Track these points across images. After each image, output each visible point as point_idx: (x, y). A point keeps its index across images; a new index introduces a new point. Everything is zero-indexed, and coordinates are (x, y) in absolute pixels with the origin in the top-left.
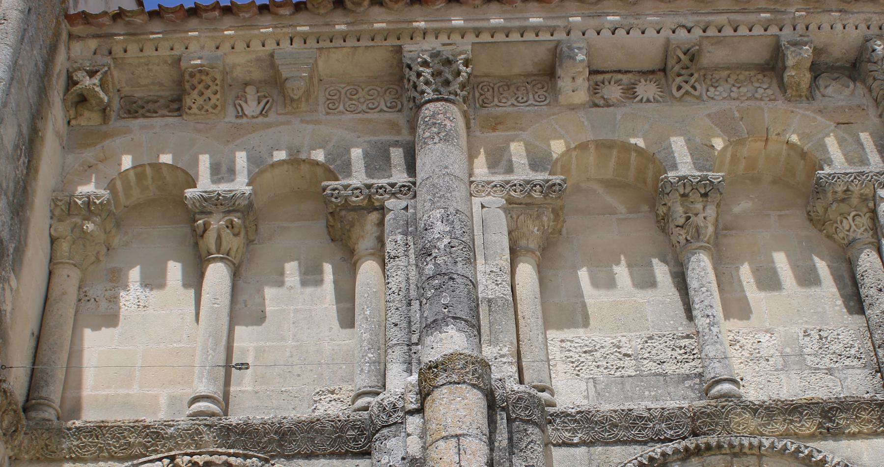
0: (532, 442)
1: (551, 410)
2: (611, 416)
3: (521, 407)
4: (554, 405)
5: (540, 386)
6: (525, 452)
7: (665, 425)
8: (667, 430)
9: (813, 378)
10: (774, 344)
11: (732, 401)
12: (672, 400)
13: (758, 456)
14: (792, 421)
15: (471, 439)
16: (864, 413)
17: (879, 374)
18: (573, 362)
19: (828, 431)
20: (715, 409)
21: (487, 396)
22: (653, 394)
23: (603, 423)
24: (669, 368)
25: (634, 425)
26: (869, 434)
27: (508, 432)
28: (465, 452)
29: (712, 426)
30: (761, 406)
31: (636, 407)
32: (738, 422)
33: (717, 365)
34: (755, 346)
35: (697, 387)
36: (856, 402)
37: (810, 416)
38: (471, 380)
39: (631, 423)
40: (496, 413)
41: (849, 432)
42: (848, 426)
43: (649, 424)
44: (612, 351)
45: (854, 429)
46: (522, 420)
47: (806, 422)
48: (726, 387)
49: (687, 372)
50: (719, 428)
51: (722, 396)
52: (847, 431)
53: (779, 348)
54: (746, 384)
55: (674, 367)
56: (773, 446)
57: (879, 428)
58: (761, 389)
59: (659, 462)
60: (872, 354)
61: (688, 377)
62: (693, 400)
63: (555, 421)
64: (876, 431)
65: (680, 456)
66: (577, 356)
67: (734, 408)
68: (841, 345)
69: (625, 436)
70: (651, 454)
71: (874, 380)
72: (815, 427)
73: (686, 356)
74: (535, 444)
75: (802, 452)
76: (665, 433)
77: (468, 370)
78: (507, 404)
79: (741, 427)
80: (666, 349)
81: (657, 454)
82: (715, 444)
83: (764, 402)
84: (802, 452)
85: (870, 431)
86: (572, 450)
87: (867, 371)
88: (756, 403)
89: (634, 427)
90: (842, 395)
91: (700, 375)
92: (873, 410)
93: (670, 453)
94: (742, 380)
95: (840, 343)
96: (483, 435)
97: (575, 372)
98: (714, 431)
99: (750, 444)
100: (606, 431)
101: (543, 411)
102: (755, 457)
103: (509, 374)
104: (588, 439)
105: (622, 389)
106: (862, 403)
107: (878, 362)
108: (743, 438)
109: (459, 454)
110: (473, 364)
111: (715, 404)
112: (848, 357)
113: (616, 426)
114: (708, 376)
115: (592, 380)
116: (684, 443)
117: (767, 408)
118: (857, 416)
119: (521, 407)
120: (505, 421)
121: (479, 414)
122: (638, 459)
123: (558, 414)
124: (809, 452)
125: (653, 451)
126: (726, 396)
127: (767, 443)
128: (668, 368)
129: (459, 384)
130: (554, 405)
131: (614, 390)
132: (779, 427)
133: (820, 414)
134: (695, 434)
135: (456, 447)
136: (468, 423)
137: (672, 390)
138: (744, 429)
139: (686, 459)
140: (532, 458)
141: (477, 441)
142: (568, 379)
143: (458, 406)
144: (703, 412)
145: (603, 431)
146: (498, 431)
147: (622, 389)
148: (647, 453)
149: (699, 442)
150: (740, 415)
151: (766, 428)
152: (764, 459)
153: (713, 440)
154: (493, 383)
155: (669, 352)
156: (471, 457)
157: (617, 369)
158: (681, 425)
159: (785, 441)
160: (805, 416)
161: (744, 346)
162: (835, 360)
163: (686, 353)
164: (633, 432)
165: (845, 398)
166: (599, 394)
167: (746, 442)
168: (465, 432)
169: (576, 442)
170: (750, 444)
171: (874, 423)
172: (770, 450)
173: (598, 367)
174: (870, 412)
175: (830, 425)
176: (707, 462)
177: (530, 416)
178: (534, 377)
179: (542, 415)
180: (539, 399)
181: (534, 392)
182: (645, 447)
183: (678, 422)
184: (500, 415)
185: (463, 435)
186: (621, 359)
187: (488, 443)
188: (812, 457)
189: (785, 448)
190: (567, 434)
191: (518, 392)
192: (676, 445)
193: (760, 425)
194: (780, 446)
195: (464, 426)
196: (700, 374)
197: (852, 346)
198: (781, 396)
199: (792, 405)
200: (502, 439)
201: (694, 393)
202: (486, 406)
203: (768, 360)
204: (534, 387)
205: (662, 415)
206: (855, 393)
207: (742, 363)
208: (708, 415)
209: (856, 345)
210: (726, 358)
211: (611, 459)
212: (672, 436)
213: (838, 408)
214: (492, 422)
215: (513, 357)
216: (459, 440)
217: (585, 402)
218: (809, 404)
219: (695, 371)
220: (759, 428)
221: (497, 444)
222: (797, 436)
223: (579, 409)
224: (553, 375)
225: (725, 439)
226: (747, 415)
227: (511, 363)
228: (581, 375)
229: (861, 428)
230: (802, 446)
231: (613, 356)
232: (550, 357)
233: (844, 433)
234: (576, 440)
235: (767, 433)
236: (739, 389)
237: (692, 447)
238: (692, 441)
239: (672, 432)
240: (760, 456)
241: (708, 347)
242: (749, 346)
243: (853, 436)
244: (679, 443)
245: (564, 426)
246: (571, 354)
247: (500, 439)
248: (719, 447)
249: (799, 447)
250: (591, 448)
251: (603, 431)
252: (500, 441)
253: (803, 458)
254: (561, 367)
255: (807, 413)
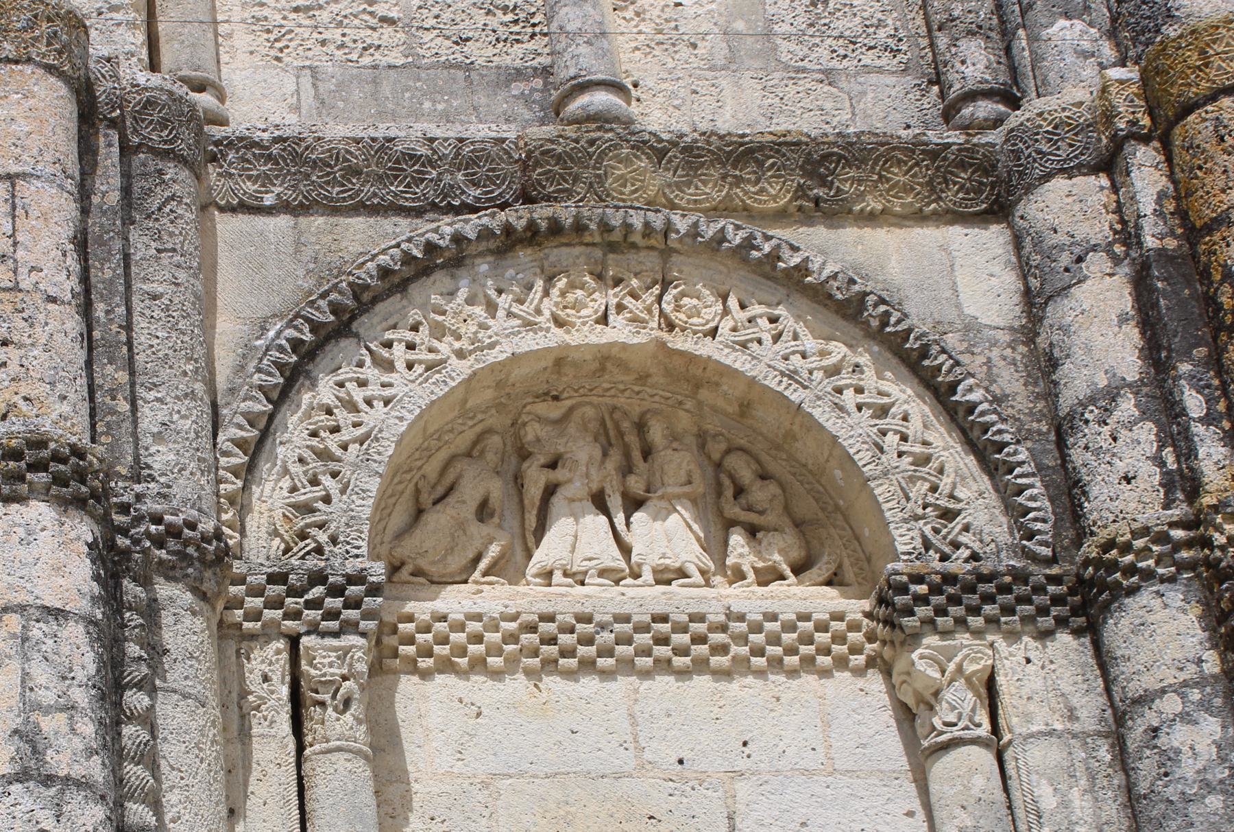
0: (172, 198)
1: (217, 132)
2: (348, 152)
3: (151, 122)
4: (223, 122)
5: (196, 78)
6: (157, 220)
7: (465, 175)
8: (467, 186)
9: (792, 89)
10: (709, 12)
11: (611, 130)
12: (481, 122)
13: (662, 252)
14: (738, 181)
15: (39, 185)
16: (896, 171)
17: (936, 89)
18: (268, 31)
19: (817, 204)
20: (573, 145)
21: (77, 92)
22: (440, 107)
23: (329, 166)
24: (479, 52)
25: (396, 174)
26: (904, 217)
27: (122, 176)
28: (26, 212)
29: (566, 181)
30: (675, 144)
31: (402, 134)
32: (622, 176)
33: (584, 49)
34: (669, 13)
35: (537, 96)
36: (882, 145)
37: (778, 170)
38: (44, 56)
39: (390, 169)
40: (97, 133)
41: (862, 210)
42: (861, 196)
43: (427, 173)
44: (354, 11)
45: (873, 203)
46: (152, 150)
47: (770, 183)
48: (600, 99)
49: (518, 63)
50: (580, 188)
51: (590, 118)
52: (857, 208)
53: (722, 21)
54: (643, 97)
55: (490, 51)
56: (694, 232)
57: (928, 204)
58: (677, 108)
59: (447, 254)
60: (924, 42)
61: (519, 74)
62: (527, 123)
63: (224, 156)
64: (921, 210)
65: (492, 244)
66: (278, 17)
67: (615, 146)
68: (857, 20)
69: (375, 195)
70: (429, 235)
71: (925, 100)
72: (789, 196)
73: (516, 29)
74: (180, 202)
75: (758, 248)
76: (463, 192)
77: (37, 33)
78: (122, 114)
79: (629, 188)
80: (474, 11)
81: (442, 238)
82: (570, 221)
83: (681, 136)
84: (758, 248)
85: (908, 210)
86: (260, 221)
87: (910, 80)
88: (665, 136)
89: (396, 177)
90: (851, 130)
91: (546, 71)
92: (917, 164)
93: (472, 235)
94: (635, 85)
95: (855, 15)
96: (67, 177)
97: (273, 53)
98: (569, 193)
99: (647, 224)
100: (335, 182)
101: (199, 132)
102: (655, 253)
103: (127, 48)
104: (295, 199)
105: (375, 95)
106: (894, 149)
107: (935, 61)
108: (631, 212)
109: (14, 217)
110: (49, 20)
111: (574, 136)
112: (871, 48)
113: (358, 173)
114: (564, 74)
115: (308, 72)
116: (502, 216)
117: (688, 149)
118: (881, 176)
119: (151, 122)
120: (116, 150)
121: (59, 130)
122: (403, 246)
123: (231, 143)
124: (773, 249)
125: (436, 231)
126: (600, 119)
127: (682, 224)
128: (476, 52)
129: (17, 62)
130: (223, 122)
131: (357, 95)
132: (711, 191)
133: (802, 168)
134: (528, 199)
135: (6, 200)
136: (35, 152)
137: (483, 100)
138: (636, 191)
139: (506, 251)
140: (171, 234)
141: (54, 191)
142: (257, 68)
143: (14, 113)
144: (548, 151)
145: (328, 183)
146: (99, 173)
147: (375, 95)
148: (423, 235)
149: (535, 216)
150: (627, 161)
151: (683, 192)
152: (675, 258)
153: (566, 212)
154: (92, 65)
155: (480, 18)
156: (40, 224)
157: (365, 49)
158: (498, 177)
159: (722, 223)
160: (769, 169)
161: (644, 11)
162: (842, 52)
163: (516, 22)
164: (392, 188)
165: (858, 135)
166: (323, 103)
167: (637, 221)
168: (28, 169)
169: (268, 203)
170: (647, 224)
171: (918, 194)
172: (688, 240)
173: (323, 43)
174: (911, 168)
175: (820, 192)
176: (552, 259)
177: (171, 142)
178: (184, 58)
179: (197, 142)
180: (193, 107)
181: (181, 90)
182: (419, 221)
183: (493, 170)
184: (106, 135)
185: (23, 176)
186: (374, 29)
187: (77, 196)
188: (779, 259)
189: (721, 237)
190: (250, 187)
191: (146, 89)
192: (485, 220)
193: (669, 186)
194: (711, 233)
195: (25, 157)
196: (545, 68)
197: (880, 24)
198: (719, 124)
199: (742, 144)
200: (108, 189)
201: (530, 109)
202: (75, 115)
203: (694, 46)
204: (182, 79)
205: (457, 154)
206: (880, 127)
207: (637, 49)
208: (559, 159)
209: (890, 22)
210: (603, 34)
211: (344, 244)
212: (477, 199)
213: (841, 157)
214: (87, 151)
215: (137, 11)
216: (13, 186)
217: (292, 119)
218: (780, 144)
219: (535, 63)
220: (667, 191)
221: (96, 200)
222: (748, 213)
223: (277, 133)
224: (224, 58)
225: (591, 212)
226: (643, 163)
227: (132, 25)
228: (286, 60)
229: (889, 201)
230: (759, 235)
231: (356, 22)
232: (220, 18)
233: (850, 211)
234: (269, 200)
235: (683, 203)
236: (629, 104)
237: (520, 225)
238: (521, 213)
239: (478, 191)
240: (667, 253)
241: (565, 10)
242: (657, 12)
243: (871, 218)
244: (493, 215)
245: (244, 169)
246: (266, 12)
247: (103, 188)
248: (579, 227)
249: (751, 237)
250: (301, 219)
251: (328, 183)
252: (104, 194)
253: (759, 261)
254: (242, 40)
255: (773, 165)
